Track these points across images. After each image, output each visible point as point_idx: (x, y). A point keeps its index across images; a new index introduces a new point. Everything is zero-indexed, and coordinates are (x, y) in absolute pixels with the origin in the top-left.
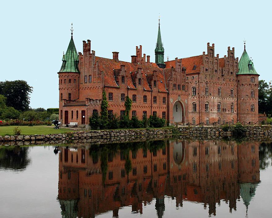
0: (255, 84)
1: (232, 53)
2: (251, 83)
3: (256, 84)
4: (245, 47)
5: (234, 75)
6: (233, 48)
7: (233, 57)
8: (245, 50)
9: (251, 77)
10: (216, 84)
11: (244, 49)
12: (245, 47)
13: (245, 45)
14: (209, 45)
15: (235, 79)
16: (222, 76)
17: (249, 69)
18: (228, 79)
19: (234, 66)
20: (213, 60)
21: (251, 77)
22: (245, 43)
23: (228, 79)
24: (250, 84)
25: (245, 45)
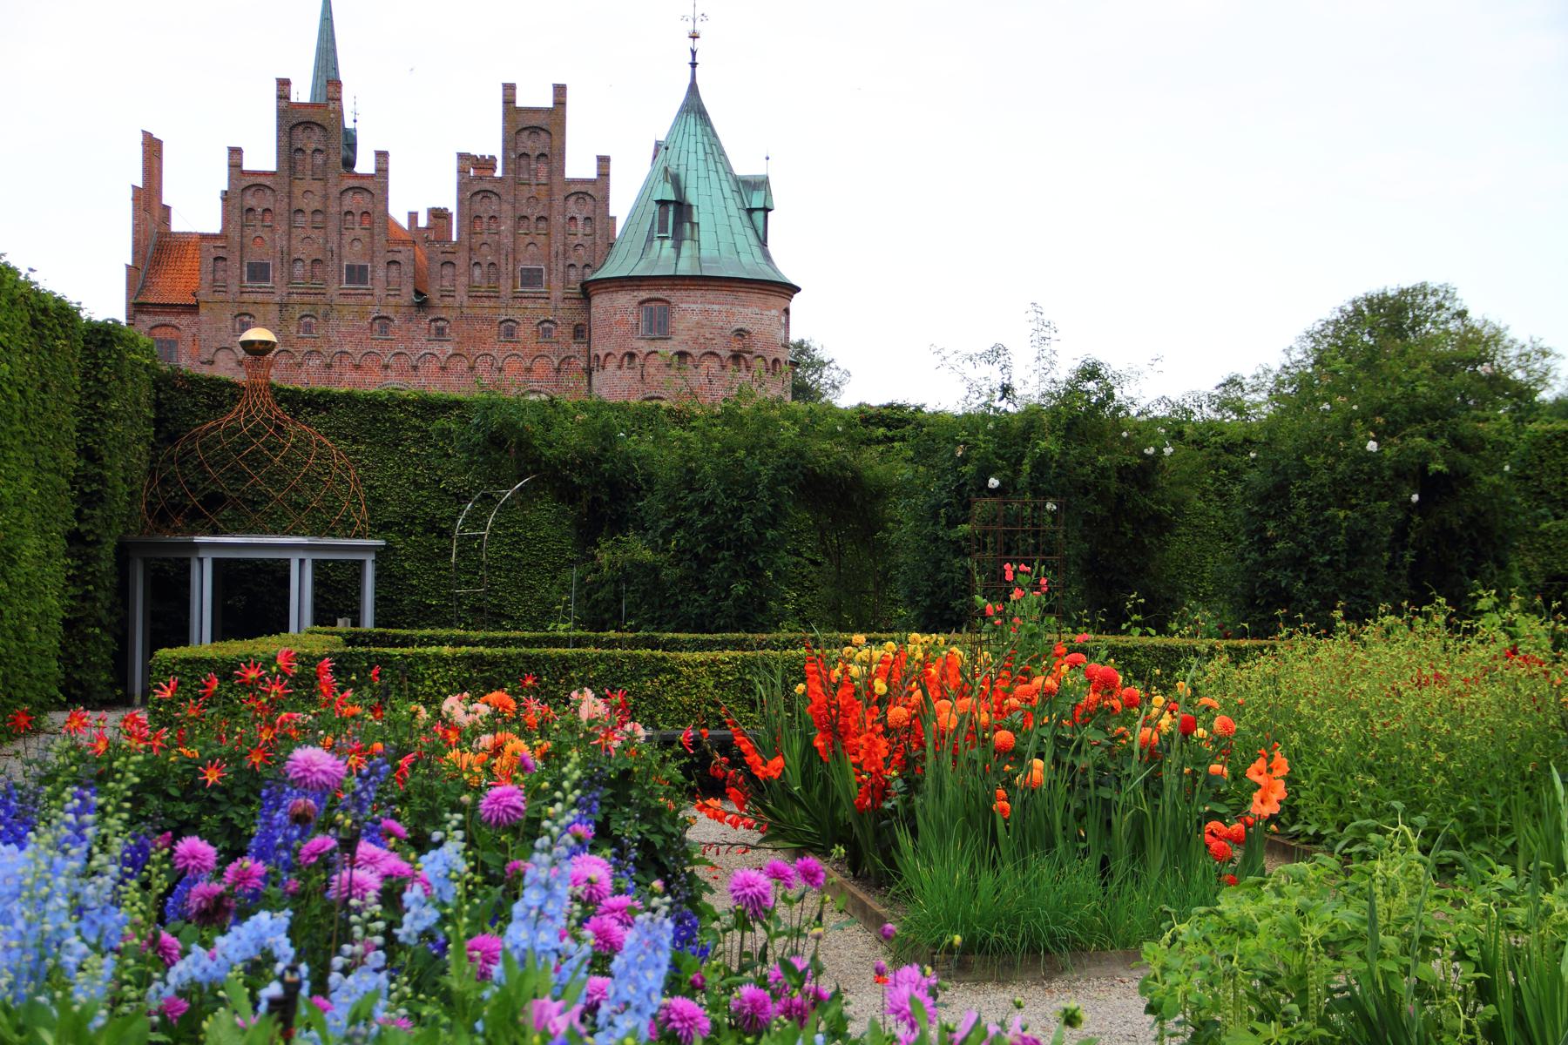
0: (668, 348)
1: (534, 130)
2: (643, 347)
3: (682, 355)
4: (694, 65)
5: (557, 293)
6: (560, 91)
7: (554, 155)
8: (693, 88)
9: (644, 295)
10: (357, 367)
11: (688, 81)
12: (694, 65)
13: (694, 53)
14: (288, 98)
15: (565, 314)
16: (422, 302)
17: (650, 240)
18: (484, 320)
19: (558, 220)
20: (326, 197)
21: (644, 295)
22: (694, 37)
23: (484, 320)
24: (632, 356)
25: (694, 53)
